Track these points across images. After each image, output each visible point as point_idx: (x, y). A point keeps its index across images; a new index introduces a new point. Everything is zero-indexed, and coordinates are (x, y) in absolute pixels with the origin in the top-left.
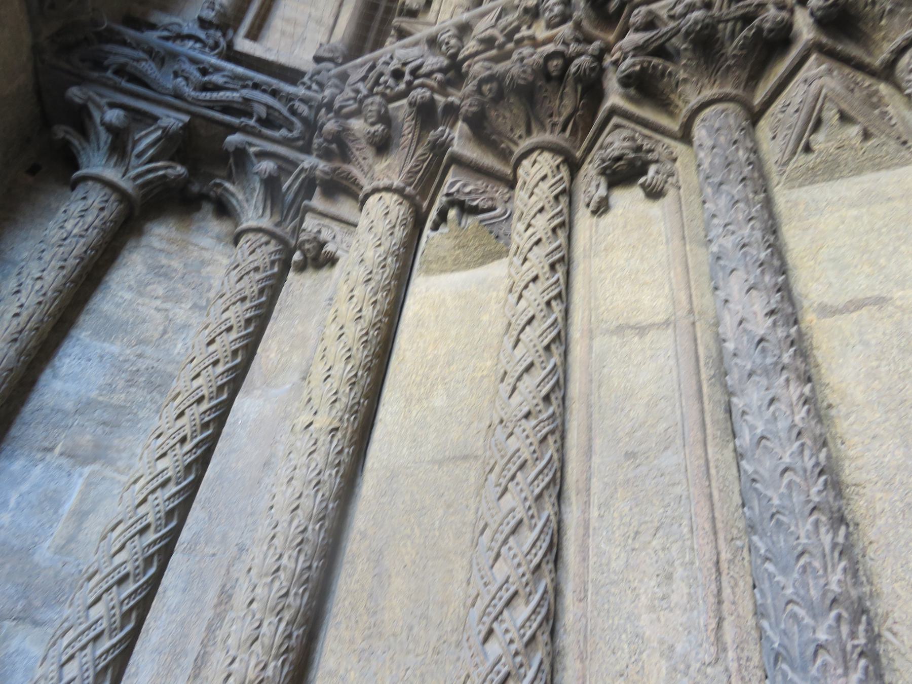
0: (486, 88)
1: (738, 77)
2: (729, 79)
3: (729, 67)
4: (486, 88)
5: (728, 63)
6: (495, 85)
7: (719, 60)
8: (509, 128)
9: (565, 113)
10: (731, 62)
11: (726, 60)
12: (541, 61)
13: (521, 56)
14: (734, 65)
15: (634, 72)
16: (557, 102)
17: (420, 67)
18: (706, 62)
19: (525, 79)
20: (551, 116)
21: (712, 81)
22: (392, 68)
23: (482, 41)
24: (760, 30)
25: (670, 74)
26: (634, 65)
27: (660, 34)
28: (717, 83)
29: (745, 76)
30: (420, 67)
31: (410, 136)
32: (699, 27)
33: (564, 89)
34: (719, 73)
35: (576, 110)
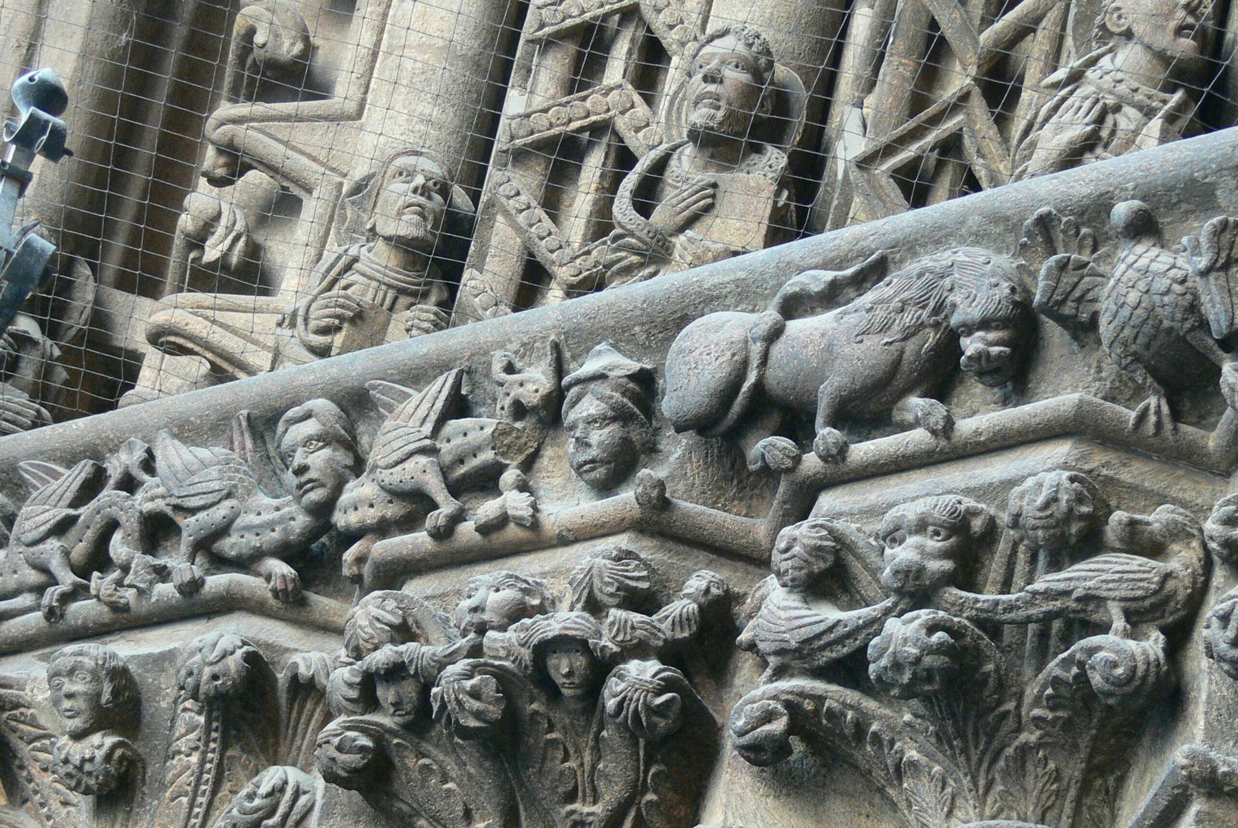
0: (386, 694)
1: (1057, 776)
2: (1030, 781)
3: (1024, 750)
4: (386, 694)
5: (1024, 737)
6: (409, 690)
7: (996, 728)
8: (459, 810)
9: (612, 794)
10: (1030, 736)
11: (1019, 730)
12: (526, 654)
13: (477, 618)
14: (1040, 745)
15: (770, 738)
16: (587, 758)
17: (223, 530)
18: (961, 734)
19: (477, 715)
20: (571, 797)
21: (982, 782)
22: (148, 507)
23: (395, 494)
24: (1083, 678)
25: (876, 738)
26: (769, 717)
27: (841, 631)
28: (999, 787)
29: (1074, 770)
30: (223, 530)
31: (195, 758)
32: (906, 678)
33: (602, 727)
34: (1002, 763)
35: (637, 789)
